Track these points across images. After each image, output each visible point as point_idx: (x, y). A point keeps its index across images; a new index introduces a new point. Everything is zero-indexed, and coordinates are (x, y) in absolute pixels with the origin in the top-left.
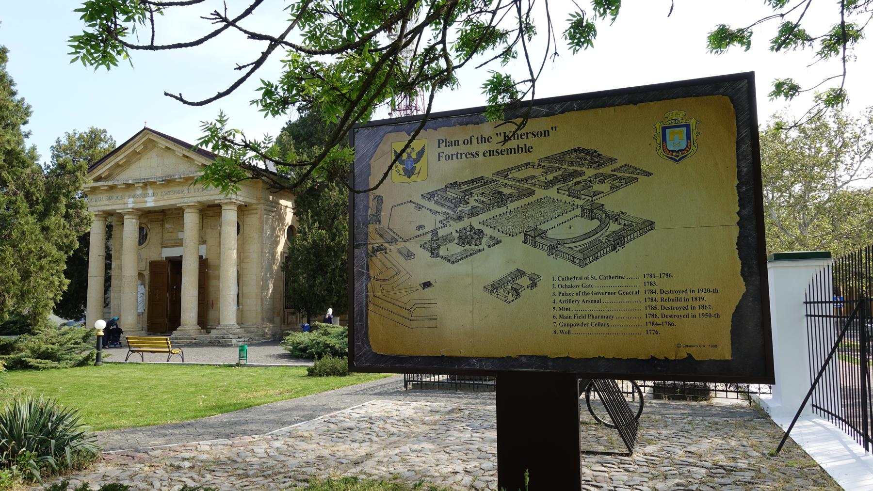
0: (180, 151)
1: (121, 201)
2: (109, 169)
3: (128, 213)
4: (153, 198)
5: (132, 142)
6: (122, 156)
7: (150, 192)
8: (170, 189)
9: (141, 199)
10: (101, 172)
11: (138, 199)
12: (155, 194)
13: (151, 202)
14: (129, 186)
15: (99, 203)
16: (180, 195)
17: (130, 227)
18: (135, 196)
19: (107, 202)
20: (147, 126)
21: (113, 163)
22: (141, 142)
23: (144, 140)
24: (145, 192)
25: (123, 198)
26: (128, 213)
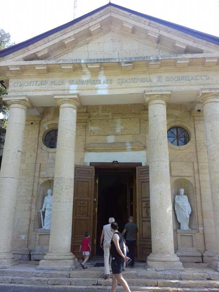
0: (154, 31)
1: (59, 87)
2: (49, 47)
3: (70, 101)
4: (106, 86)
5: (88, 18)
6: (72, 33)
7: (102, 78)
8: (133, 76)
9: (90, 86)
10: (39, 49)
11: (85, 86)
12: (109, 81)
13: (103, 89)
14: (77, 67)
15: (25, 88)
16: (146, 84)
17: (68, 119)
18: (81, 82)
19: (37, 87)
20: (112, 2)
21: (57, 41)
22: (99, 20)
23: (103, 18)
24: (94, 78)
25: (63, 83)
26: (70, 101)
